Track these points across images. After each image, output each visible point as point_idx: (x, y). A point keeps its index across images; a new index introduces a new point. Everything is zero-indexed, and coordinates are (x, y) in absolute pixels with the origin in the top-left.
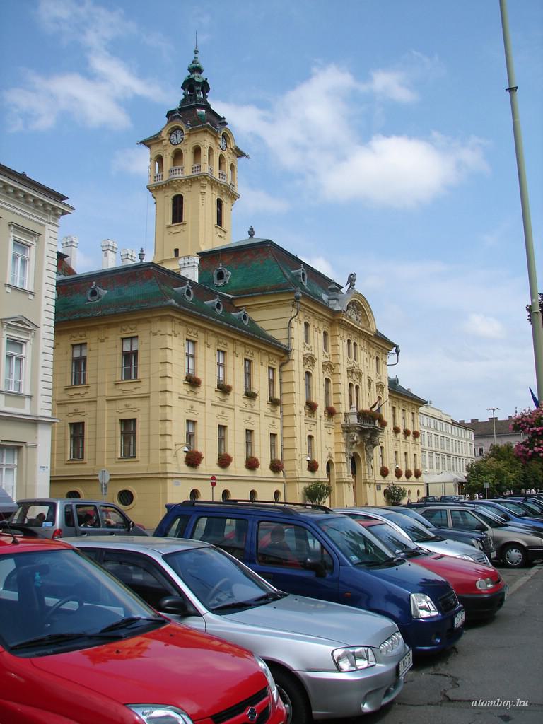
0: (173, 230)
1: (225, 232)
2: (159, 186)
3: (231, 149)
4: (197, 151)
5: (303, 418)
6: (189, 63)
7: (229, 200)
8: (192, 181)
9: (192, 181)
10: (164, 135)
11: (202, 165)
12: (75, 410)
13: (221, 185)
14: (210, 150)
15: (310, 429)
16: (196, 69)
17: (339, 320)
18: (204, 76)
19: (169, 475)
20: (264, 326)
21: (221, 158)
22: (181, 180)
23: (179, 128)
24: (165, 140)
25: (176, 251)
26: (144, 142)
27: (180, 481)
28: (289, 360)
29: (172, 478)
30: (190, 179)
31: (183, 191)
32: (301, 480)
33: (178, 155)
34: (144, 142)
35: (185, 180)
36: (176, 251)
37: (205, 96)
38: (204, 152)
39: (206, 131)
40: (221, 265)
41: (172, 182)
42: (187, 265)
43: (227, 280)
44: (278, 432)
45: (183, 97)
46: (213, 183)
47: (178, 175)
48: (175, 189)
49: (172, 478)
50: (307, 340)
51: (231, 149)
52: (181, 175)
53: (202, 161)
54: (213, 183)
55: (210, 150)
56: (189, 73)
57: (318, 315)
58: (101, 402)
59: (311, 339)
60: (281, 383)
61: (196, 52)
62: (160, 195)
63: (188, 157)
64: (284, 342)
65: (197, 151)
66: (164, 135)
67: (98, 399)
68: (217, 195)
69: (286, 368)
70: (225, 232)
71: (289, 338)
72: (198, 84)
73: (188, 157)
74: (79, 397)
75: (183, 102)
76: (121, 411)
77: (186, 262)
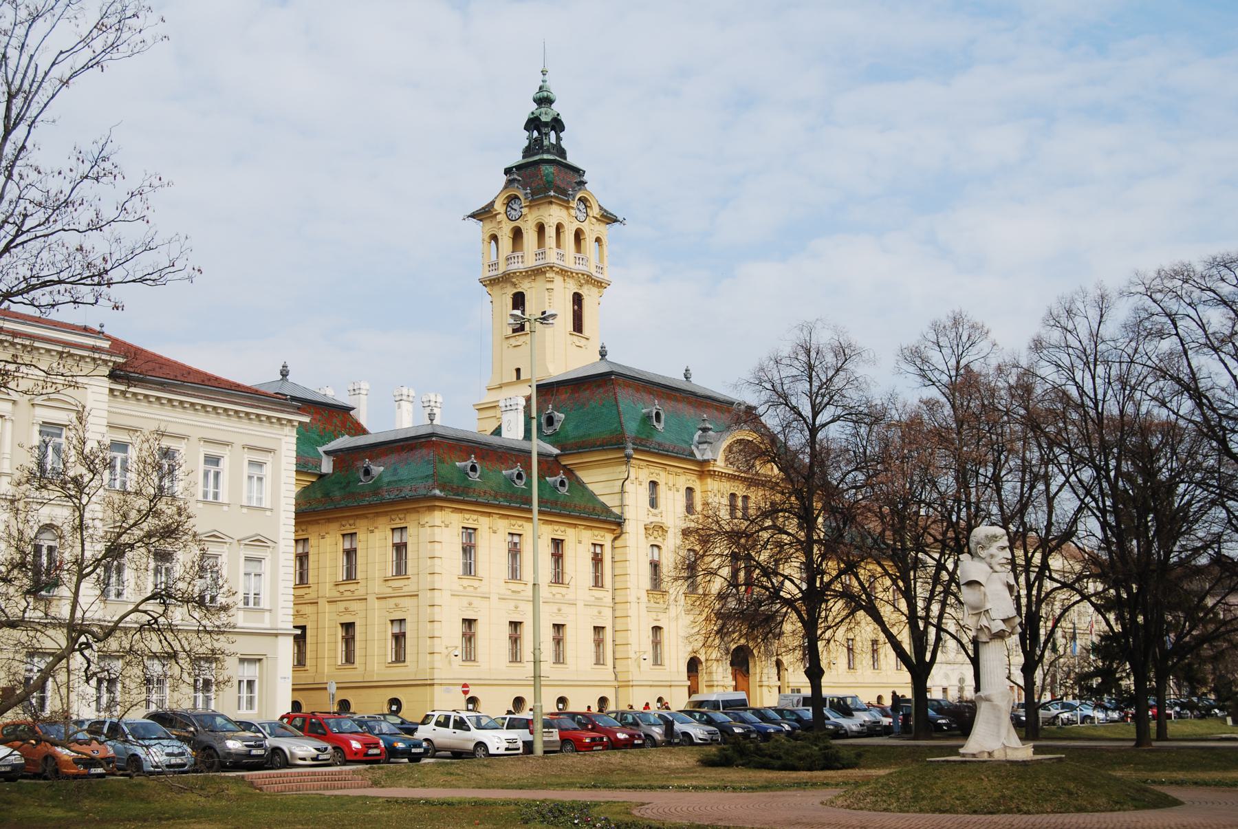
0: (513, 342)
1: (587, 339)
2: (494, 280)
3: (594, 217)
4: (541, 229)
5: (643, 606)
6: (533, 91)
7: (595, 290)
8: (536, 273)
9: (536, 273)
10: (499, 207)
11: (547, 251)
12: (345, 608)
13: (577, 274)
14: (559, 228)
15: (655, 617)
16: (544, 101)
17: (709, 471)
18: (556, 108)
19: (436, 682)
20: (595, 489)
21: (578, 235)
22: (521, 273)
23: (516, 197)
24: (499, 213)
25: (518, 370)
26: (473, 216)
27: (451, 687)
28: (622, 533)
29: (441, 684)
30: (533, 271)
31: (525, 286)
32: (634, 683)
33: (517, 234)
34: (473, 216)
35: (527, 272)
36: (518, 370)
37: (559, 139)
38: (550, 232)
39: (551, 203)
40: (550, 406)
41: (509, 274)
42: (509, 408)
43: (557, 426)
44: (606, 622)
45: (526, 143)
46: (564, 272)
47: (517, 266)
48: (514, 285)
49: (441, 684)
50: (653, 503)
51: (594, 217)
52: (521, 266)
53: (547, 246)
54: (564, 272)
55: (559, 228)
56: (535, 106)
57: (672, 469)
58: (372, 599)
59: (662, 501)
60: (613, 562)
61: (544, 73)
62: (496, 290)
63: (530, 237)
64: (617, 511)
65: (541, 229)
66: (499, 207)
67: (368, 597)
68: (572, 287)
69: (617, 543)
70: (587, 339)
71: (622, 506)
72: (546, 124)
73: (530, 237)
74: (349, 593)
75: (528, 152)
76: (391, 611)
77: (508, 404)
